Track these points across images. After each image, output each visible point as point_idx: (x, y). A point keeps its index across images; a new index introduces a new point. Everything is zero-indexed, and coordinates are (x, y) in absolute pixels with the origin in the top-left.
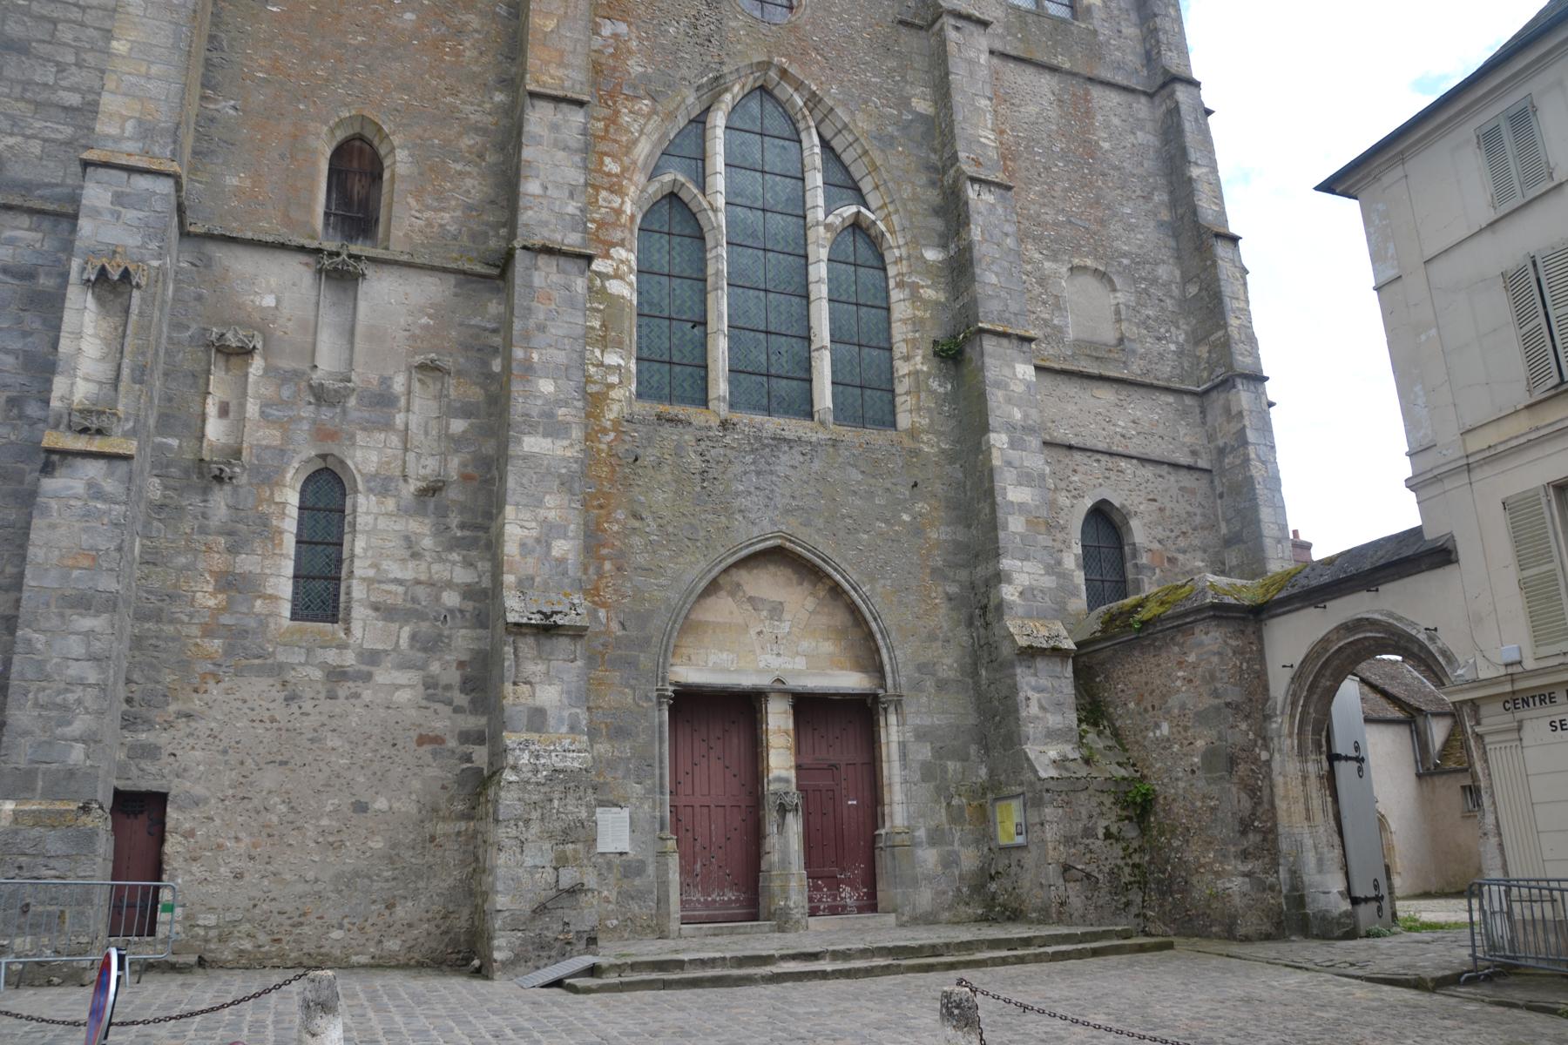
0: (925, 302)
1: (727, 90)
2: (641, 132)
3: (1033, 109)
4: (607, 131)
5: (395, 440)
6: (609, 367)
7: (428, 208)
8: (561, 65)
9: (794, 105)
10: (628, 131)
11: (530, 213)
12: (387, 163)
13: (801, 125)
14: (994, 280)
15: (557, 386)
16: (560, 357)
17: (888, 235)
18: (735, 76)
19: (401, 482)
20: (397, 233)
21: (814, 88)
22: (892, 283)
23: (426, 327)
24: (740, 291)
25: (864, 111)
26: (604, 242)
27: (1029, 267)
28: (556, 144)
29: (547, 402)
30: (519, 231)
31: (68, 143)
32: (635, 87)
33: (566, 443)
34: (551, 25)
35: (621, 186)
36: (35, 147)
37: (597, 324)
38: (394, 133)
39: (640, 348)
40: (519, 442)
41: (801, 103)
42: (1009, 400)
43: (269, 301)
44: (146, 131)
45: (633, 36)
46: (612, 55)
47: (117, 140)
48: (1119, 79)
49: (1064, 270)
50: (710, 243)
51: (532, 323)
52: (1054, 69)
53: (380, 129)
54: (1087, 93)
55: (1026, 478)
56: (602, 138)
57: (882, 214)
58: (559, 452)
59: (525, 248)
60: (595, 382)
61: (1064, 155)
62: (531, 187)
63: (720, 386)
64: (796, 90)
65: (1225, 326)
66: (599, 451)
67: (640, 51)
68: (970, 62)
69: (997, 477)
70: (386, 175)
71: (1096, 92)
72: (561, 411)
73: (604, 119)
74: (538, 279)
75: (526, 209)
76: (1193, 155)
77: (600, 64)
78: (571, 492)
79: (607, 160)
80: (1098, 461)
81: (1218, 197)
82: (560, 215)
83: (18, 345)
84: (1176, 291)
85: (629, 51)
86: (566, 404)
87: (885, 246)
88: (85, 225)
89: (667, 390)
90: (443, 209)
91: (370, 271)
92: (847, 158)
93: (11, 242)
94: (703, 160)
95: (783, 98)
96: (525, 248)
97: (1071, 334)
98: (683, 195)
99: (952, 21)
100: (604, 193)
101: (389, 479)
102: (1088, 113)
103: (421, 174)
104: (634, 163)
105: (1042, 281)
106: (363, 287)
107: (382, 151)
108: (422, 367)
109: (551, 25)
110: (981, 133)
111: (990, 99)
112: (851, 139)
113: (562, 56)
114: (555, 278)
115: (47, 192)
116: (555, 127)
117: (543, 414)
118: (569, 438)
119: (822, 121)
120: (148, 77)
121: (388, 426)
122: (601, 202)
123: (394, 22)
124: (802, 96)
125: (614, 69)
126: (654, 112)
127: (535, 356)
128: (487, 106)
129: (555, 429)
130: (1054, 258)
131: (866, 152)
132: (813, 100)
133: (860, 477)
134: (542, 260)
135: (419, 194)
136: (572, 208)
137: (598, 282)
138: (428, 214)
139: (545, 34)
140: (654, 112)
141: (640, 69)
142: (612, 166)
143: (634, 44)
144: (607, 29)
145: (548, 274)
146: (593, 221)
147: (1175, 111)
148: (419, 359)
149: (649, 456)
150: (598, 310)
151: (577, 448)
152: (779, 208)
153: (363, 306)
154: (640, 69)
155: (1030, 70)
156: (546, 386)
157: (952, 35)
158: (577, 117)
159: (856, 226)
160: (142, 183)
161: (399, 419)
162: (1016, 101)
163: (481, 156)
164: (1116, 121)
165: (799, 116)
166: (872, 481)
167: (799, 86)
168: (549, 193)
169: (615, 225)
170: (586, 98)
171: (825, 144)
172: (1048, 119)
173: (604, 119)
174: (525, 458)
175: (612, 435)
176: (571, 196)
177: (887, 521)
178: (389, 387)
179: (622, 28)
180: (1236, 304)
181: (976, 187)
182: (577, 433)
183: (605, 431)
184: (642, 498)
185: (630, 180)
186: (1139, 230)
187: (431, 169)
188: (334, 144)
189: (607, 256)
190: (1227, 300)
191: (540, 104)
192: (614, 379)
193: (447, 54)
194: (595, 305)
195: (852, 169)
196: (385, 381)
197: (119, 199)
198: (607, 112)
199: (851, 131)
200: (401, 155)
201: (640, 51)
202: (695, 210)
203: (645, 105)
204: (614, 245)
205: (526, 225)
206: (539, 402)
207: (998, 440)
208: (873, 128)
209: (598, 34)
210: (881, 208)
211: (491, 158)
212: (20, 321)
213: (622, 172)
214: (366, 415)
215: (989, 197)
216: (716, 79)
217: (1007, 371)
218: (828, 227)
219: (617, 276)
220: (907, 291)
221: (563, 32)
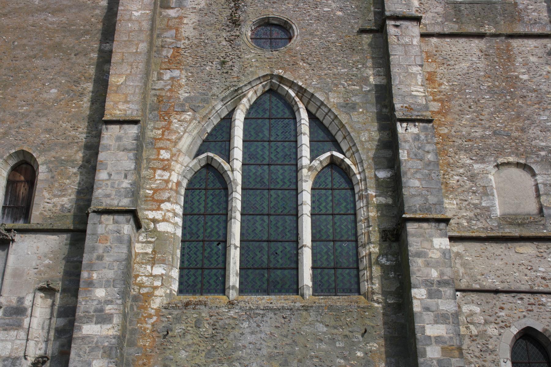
1: (244, 96)
2: (185, 132)
3: (465, 65)
4: (163, 134)
5: (22, 334)
6: (155, 276)
7: (55, 196)
8: (126, 102)
9: (290, 96)
10: (176, 132)
11: (100, 191)
14: (417, 183)
15: (107, 292)
16: (110, 274)
17: (353, 167)
18: (249, 87)
19: (23, 359)
21: (300, 84)
23: (48, 266)
24: (250, 217)
25: (335, 91)
26: (157, 201)
27: (461, 171)
28: (119, 149)
29: (100, 302)
30: (94, 201)
32: (182, 105)
33: (109, 326)
34: (121, 80)
35: (170, 165)
37: (149, 250)
38: (39, 157)
39: (182, 262)
40: (80, 329)
41: (293, 94)
42: (428, 265)
45: (183, 76)
46: (170, 90)
48: (536, 30)
51: (95, 255)
53: (32, 156)
54: (509, 45)
55: (441, 318)
56: (160, 139)
58: (105, 333)
59: (94, 212)
60: (145, 287)
61: (490, 90)
62: (102, 175)
63: (234, 280)
64: (290, 87)
66: (145, 329)
67: (187, 85)
68: (405, 45)
69: (417, 320)
71: (515, 43)
72: (109, 307)
73: (162, 128)
74: (100, 229)
75: (98, 189)
77: (162, 96)
78: (109, 356)
79: (162, 152)
80: (522, 299)
82: (118, 191)
85: (180, 86)
86: (110, 302)
87: (351, 174)
89: (199, 286)
90: (64, 195)
91: (17, 237)
92: (326, 122)
94: (230, 141)
95: (284, 94)
96: (94, 212)
97: (498, 211)
98: (214, 164)
99: (393, 23)
100: (159, 172)
101: (17, 358)
102: (510, 59)
103: (53, 177)
104: (179, 151)
105: (472, 178)
106: (13, 247)
108: (41, 289)
110: (413, 88)
111: (421, 66)
112: (326, 111)
113: (126, 97)
114: (112, 227)
117: (95, 311)
118: (111, 323)
119: (308, 103)
121: (18, 326)
122: (157, 177)
123: (45, 96)
124: (294, 90)
125: (170, 97)
126: (194, 118)
127: (95, 275)
128: (94, 133)
129: (102, 318)
130: (482, 160)
131: (336, 117)
132: (301, 91)
133: (325, 329)
134: (104, 217)
135: (50, 188)
136: (126, 184)
137: (152, 226)
138: (55, 200)
139: (118, 86)
140: (194, 118)
141: (187, 95)
143: (183, 81)
144: (167, 76)
145: (107, 225)
146: (151, 189)
148: (41, 284)
149: (178, 329)
150: (150, 242)
151: (116, 329)
152: (279, 162)
153: (11, 258)
154: (187, 95)
155: (462, 40)
156: (100, 293)
158: (133, 130)
159: (333, 163)
161: (26, 321)
162: (452, 62)
164: (533, 59)
165: (293, 103)
166: (336, 331)
167: (292, 85)
168: (112, 177)
169: (164, 190)
170: (138, 118)
171: (312, 117)
172: (477, 69)
173: (162, 128)
174: (83, 338)
175: (155, 318)
176: (126, 177)
177: (345, 358)
178: (22, 303)
179: (176, 73)
181: (404, 125)
182: (116, 320)
183: (150, 316)
184: (171, 357)
185: (176, 161)
187: (59, 174)
188: (9, 168)
189: (159, 209)
191: (111, 127)
192: (158, 283)
193: (73, 108)
194: (150, 239)
195: (330, 129)
196: (21, 300)
198: (164, 123)
199: (326, 106)
201: (187, 85)
202: (222, 172)
203: (187, 116)
204: (163, 202)
205: (97, 198)
206: (95, 303)
207: (419, 294)
208: (341, 100)
209: (162, 79)
210: (348, 150)
213: (171, 157)
214: (7, 321)
215: (413, 129)
216: (236, 91)
217: (426, 245)
219: (164, 220)
220: (365, 200)
221: (128, 83)
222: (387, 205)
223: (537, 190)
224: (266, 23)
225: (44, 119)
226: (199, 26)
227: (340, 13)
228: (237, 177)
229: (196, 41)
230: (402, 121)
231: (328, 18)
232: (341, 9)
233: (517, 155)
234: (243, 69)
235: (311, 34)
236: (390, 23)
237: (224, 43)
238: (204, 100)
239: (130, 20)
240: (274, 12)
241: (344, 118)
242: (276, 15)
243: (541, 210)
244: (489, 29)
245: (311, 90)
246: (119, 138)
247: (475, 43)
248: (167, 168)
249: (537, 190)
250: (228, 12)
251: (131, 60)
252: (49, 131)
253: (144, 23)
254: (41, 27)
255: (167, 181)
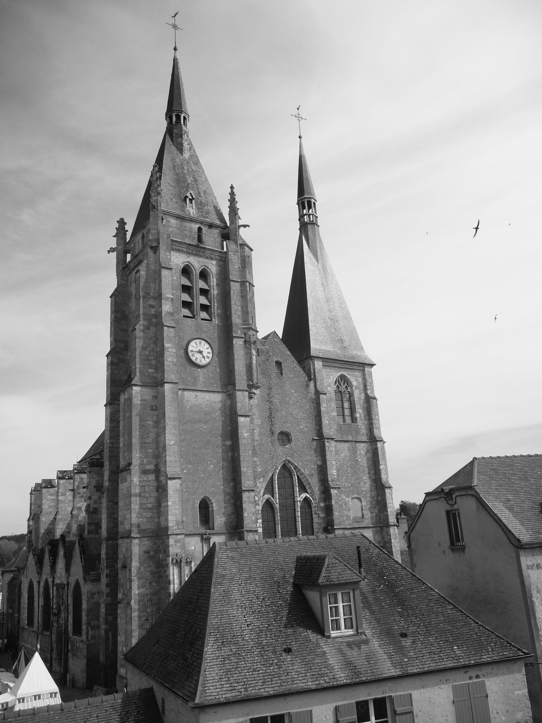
0: (321, 518)
3: (343, 454)
7: (221, 517)
8: (249, 480)
12: (210, 506)
13: (293, 474)
20: (215, 525)
22: (313, 513)
31: (150, 518)
32: (259, 475)
36: (145, 520)
43: (193, 548)
44: (177, 523)
47: (173, 527)
49: (350, 500)
50: (276, 512)
52: (348, 441)
54: (356, 446)
57: (311, 495)
65: (387, 512)
70: (210, 509)
71: (358, 444)
76: (381, 462)
81: (387, 474)
83: (149, 570)
84: (376, 499)
88: (171, 549)
93: (144, 545)
107: (209, 503)
109: (245, 469)
114: (252, 537)
115: (149, 531)
116: (249, 498)
120: (176, 509)
126: (264, 481)
130: (348, 497)
132: (296, 468)
142: (257, 499)
147: (376, 449)
157: (327, 444)
160: (179, 537)
163: (230, 501)
164: (362, 452)
167: (293, 464)
180: (390, 505)
186: (366, 484)
190: (388, 505)
197: (176, 541)
200: (214, 505)
211: (232, 501)
212: (148, 563)
215: (336, 491)
218: (300, 501)
222: (324, 517)
223: (362, 508)
224: (282, 433)
225: (211, 481)
226: (260, 434)
227: (306, 429)
228: (278, 506)
229: (260, 442)
230: (332, 488)
231: (302, 431)
232: (306, 427)
233: (358, 494)
234: (277, 457)
235: (298, 440)
236: (326, 440)
237: (270, 444)
238: (266, 473)
239: (244, 438)
240: (285, 430)
241: (310, 480)
242: (286, 430)
243: (363, 515)
244: (350, 438)
245: (299, 468)
246: (249, 498)
247: (346, 445)
248: (258, 505)
249: (362, 508)
250: (269, 427)
251: (247, 459)
252: (213, 487)
253: (249, 440)
254: (201, 431)
255: (258, 510)
